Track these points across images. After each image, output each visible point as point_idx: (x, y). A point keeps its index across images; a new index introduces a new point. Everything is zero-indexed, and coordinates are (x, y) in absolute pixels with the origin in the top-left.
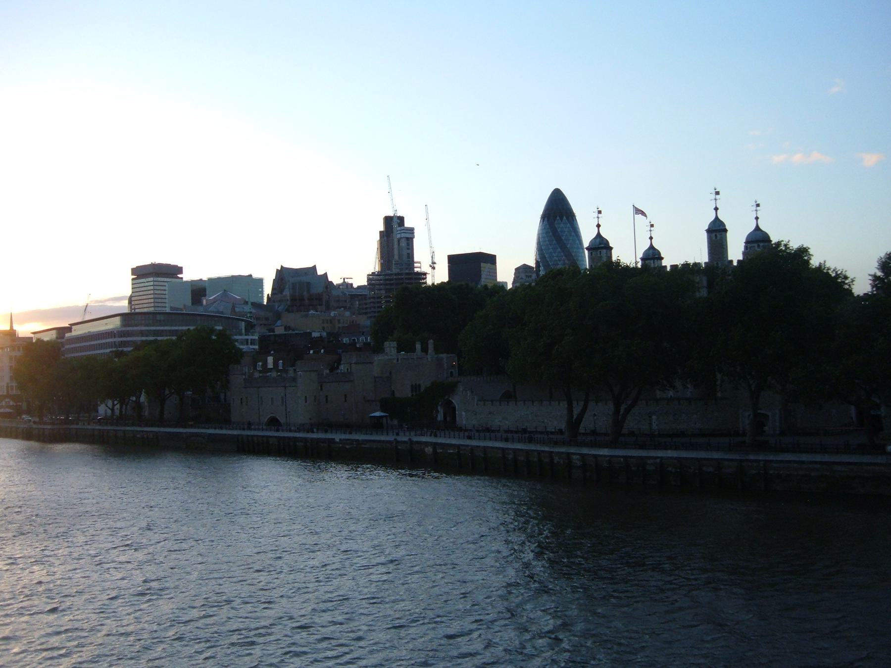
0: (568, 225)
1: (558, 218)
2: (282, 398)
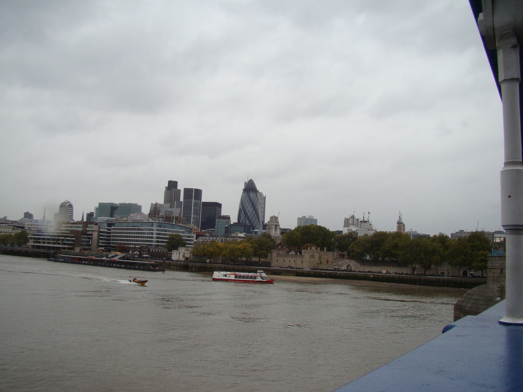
0: (255, 195)
1: (251, 191)
2: (295, 261)
